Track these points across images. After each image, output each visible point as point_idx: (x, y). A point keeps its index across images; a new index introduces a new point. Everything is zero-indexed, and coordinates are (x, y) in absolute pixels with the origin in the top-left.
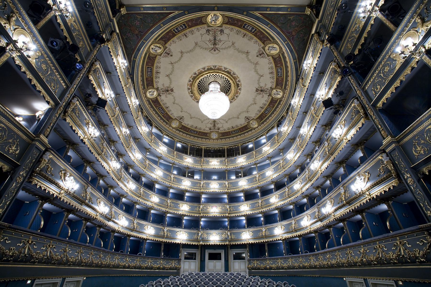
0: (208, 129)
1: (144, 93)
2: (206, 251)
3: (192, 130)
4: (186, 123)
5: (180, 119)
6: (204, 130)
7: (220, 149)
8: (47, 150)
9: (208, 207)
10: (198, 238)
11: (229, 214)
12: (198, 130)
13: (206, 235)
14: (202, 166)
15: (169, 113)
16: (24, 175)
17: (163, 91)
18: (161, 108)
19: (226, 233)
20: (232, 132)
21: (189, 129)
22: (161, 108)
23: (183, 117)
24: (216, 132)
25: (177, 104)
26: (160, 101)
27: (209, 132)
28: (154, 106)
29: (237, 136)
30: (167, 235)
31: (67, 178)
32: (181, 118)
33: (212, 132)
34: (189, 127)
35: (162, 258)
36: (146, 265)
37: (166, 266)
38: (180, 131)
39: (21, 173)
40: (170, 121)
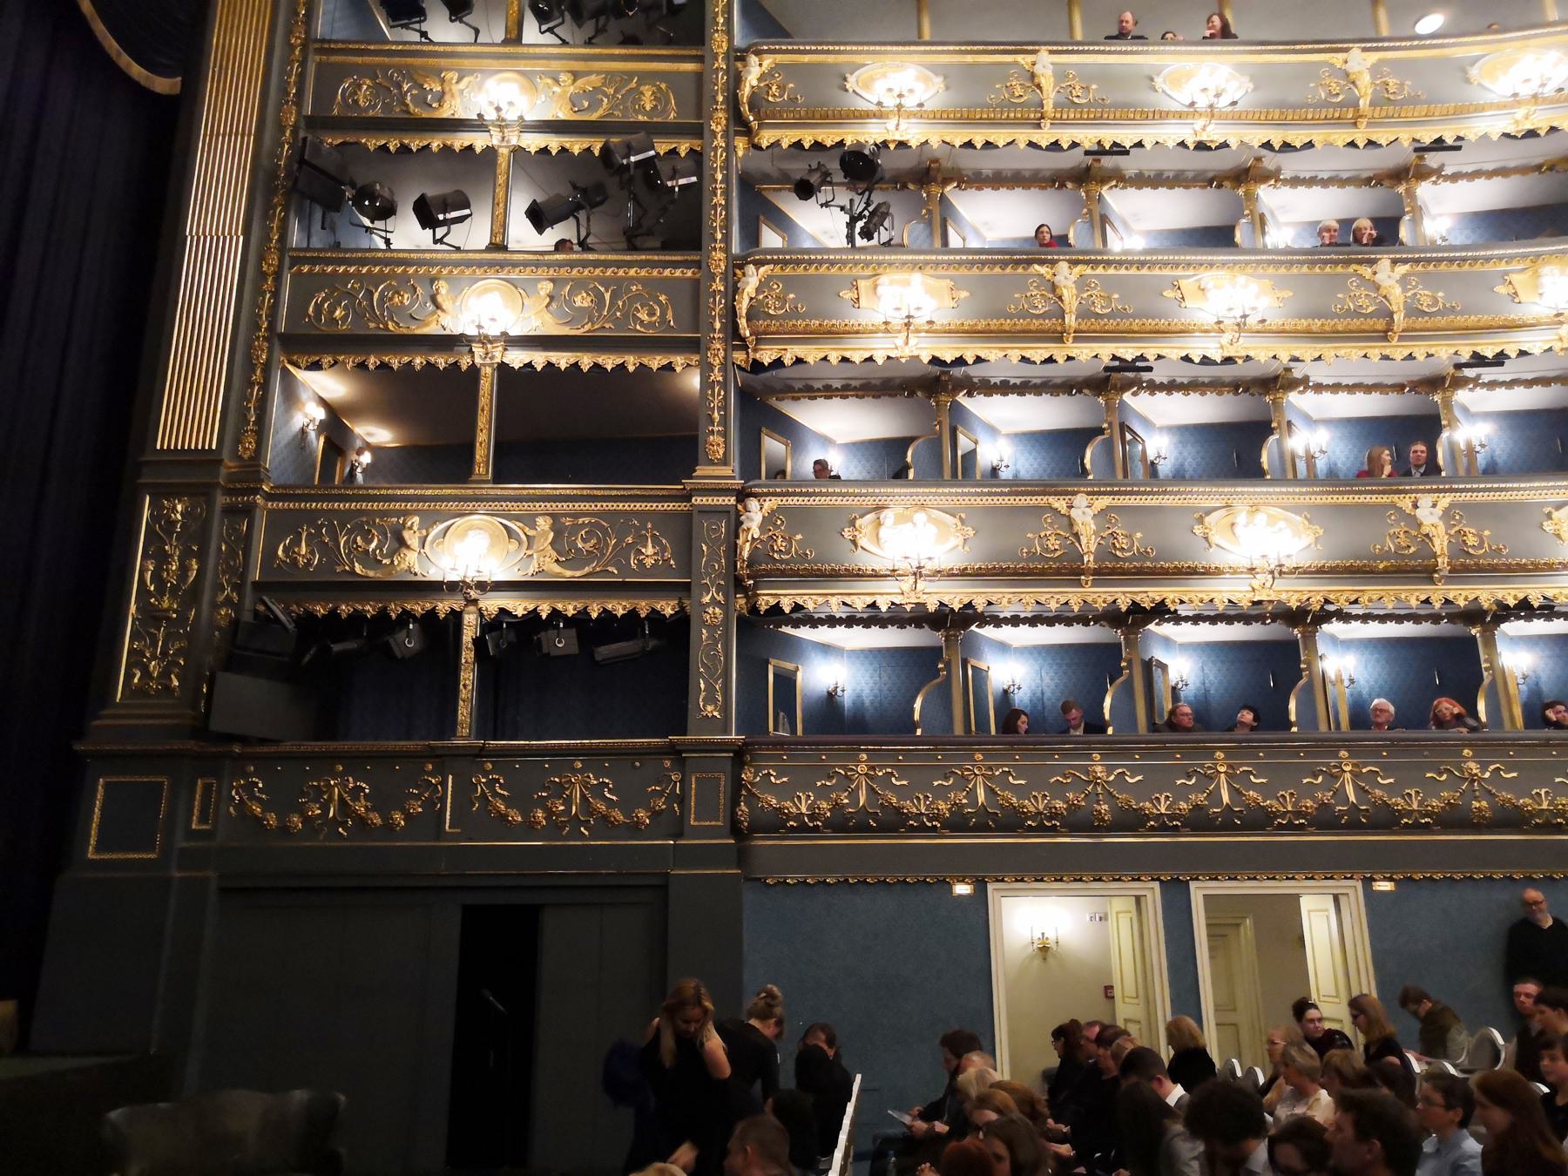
8: (743, 495)
16: (720, 598)
31: (883, 532)
39: (707, 599)
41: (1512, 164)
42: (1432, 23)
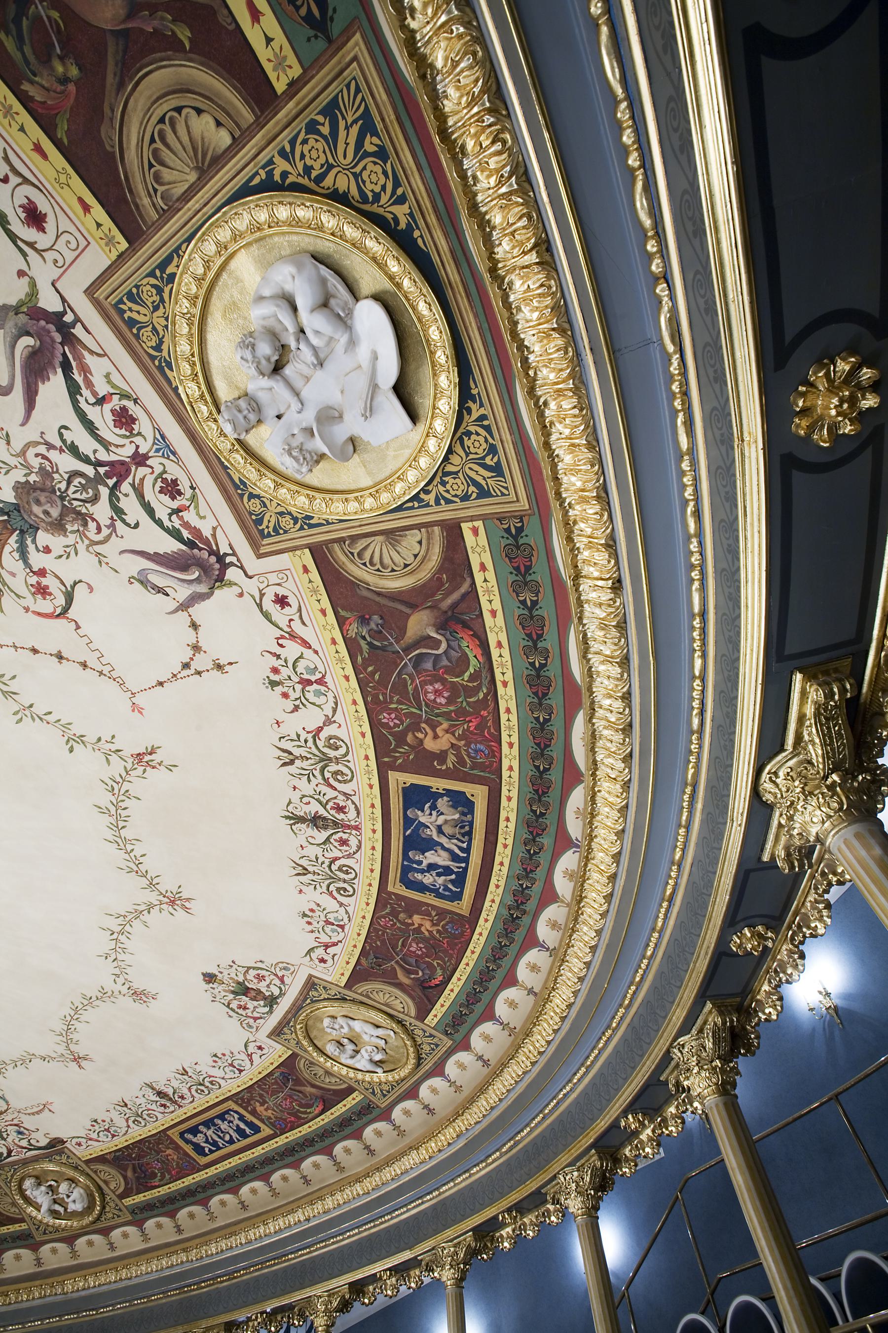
22: (194, 1131)
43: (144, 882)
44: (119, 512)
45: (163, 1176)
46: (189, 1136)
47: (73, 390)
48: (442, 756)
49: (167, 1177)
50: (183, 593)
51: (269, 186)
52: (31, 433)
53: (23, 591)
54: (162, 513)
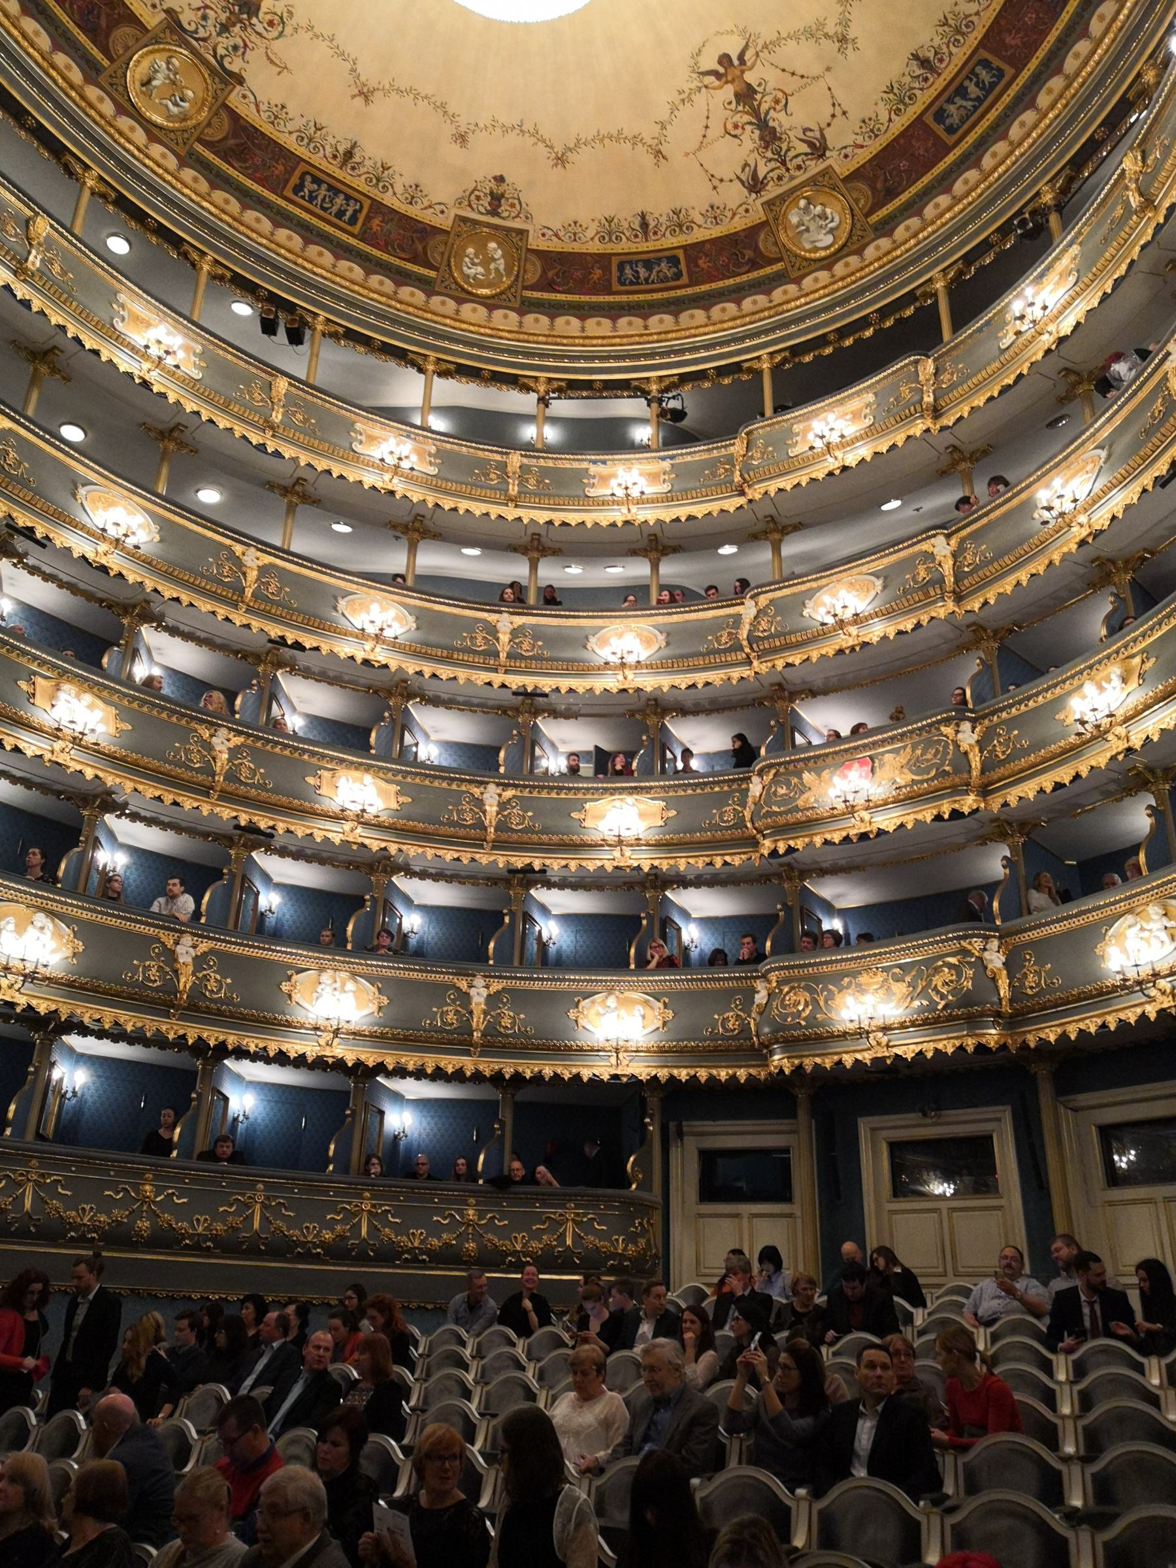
0: (735, 194)
1: (121, 110)
2: (864, 1126)
3: (627, 261)
4: (556, 225)
5: (494, 212)
6: (715, 213)
7: (900, 322)
9: (806, 776)
10: (745, 1028)
11: (985, 792)
12: (671, 241)
13: (803, 996)
14: (742, 493)
15: (388, 199)
17: (225, 28)
18: (317, 181)
19: (965, 952)
20: (940, 116)
21: (603, 259)
22: (317, 181)
23: (500, 179)
24: (813, 181)
25: (386, 93)
26: (267, 129)
27: (758, 214)
28: (256, 187)
29: (999, 130)
30: (491, 1031)
32: (496, 199)
33: (782, 198)
34: (595, 247)
35: (474, 1193)
36: (328, 1235)
37: (505, 1245)
38: (553, 310)
40: (435, 257)
41: (82, 586)
42: (72, 433)
43: (572, 146)
44: (770, 160)
45: (247, 168)
46: (308, 178)
47: (806, 154)
48: (697, 266)
49: (250, 172)
50: (744, 178)
51: (853, 215)
52: (793, 138)
53: (734, 120)
54: (771, 174)
